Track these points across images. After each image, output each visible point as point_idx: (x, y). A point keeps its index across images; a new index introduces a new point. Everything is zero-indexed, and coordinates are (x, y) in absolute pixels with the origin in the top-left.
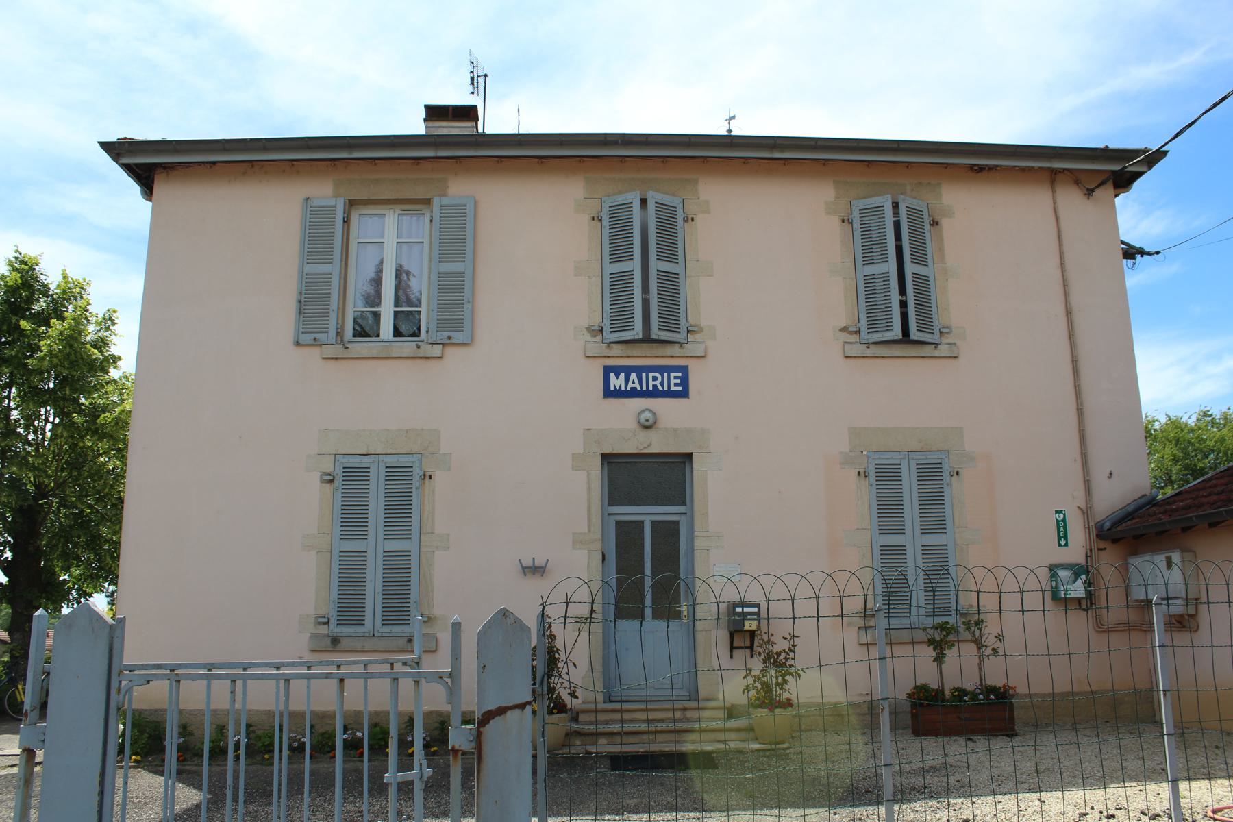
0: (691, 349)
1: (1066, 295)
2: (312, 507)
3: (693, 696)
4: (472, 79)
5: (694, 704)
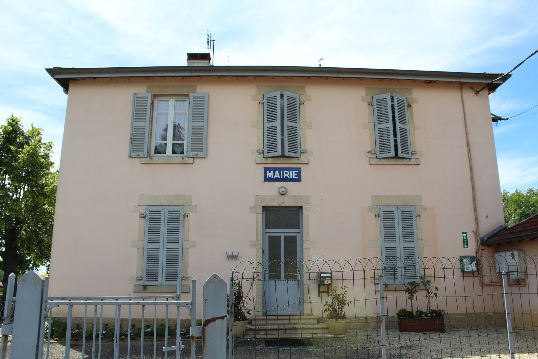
0: (302, 160)
1: (467, 138)
2: (136, 228)
4: (208, 42)
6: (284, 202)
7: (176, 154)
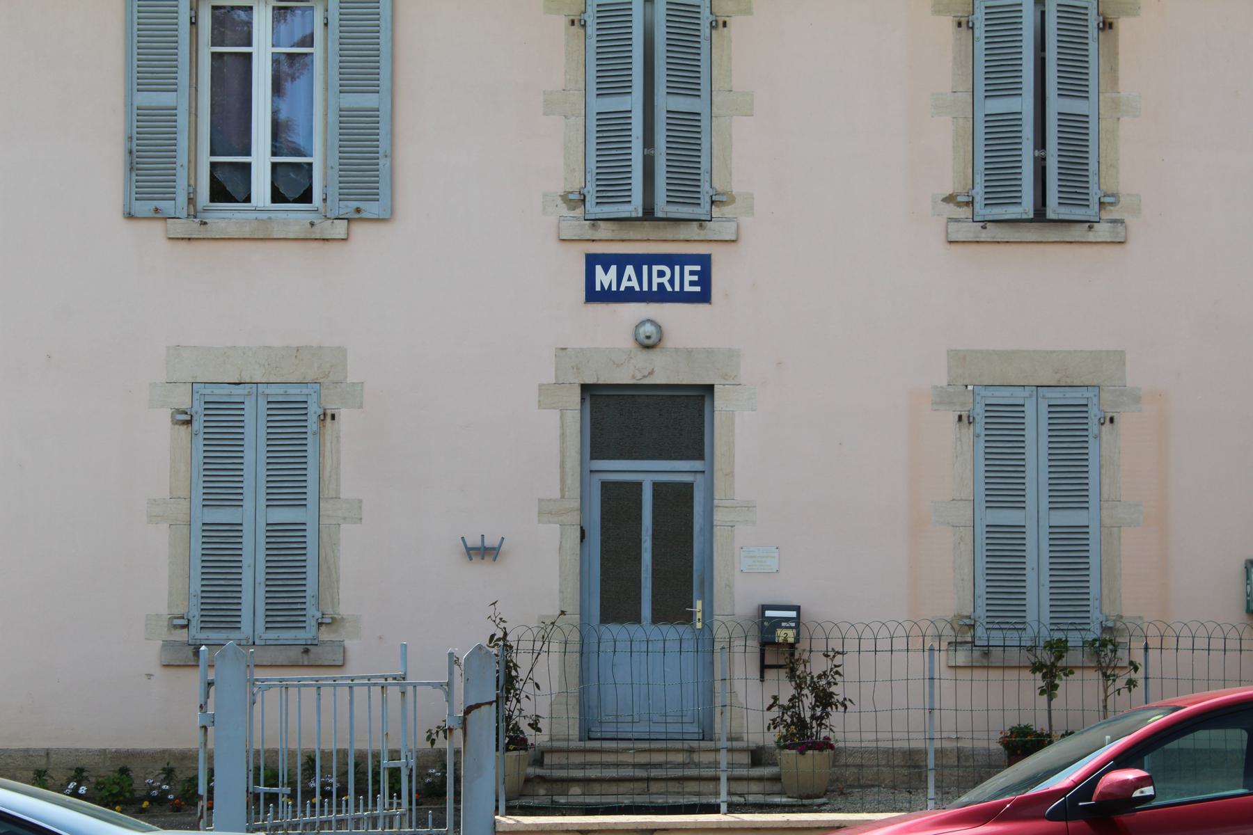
0: (716, 229)
2: (160, 461)
3: (707, 734)
5: (710, 745)
6: (651, 373)
7: (286, 200)
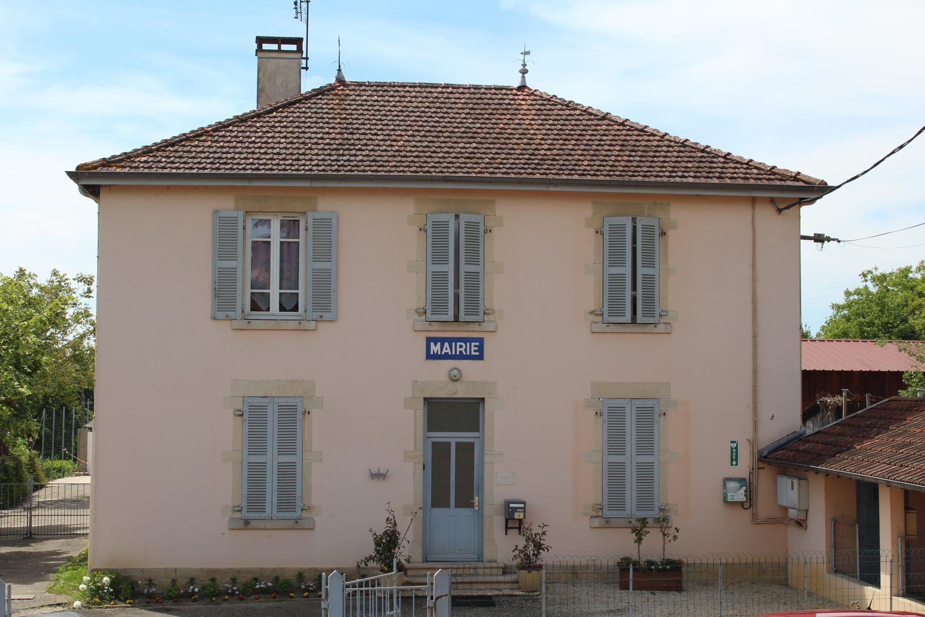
0: (487, 326)
1: (754, 287)
2: (228, 432)
3: (480, 559)
5: (480, 564)
7: (285, 310)
